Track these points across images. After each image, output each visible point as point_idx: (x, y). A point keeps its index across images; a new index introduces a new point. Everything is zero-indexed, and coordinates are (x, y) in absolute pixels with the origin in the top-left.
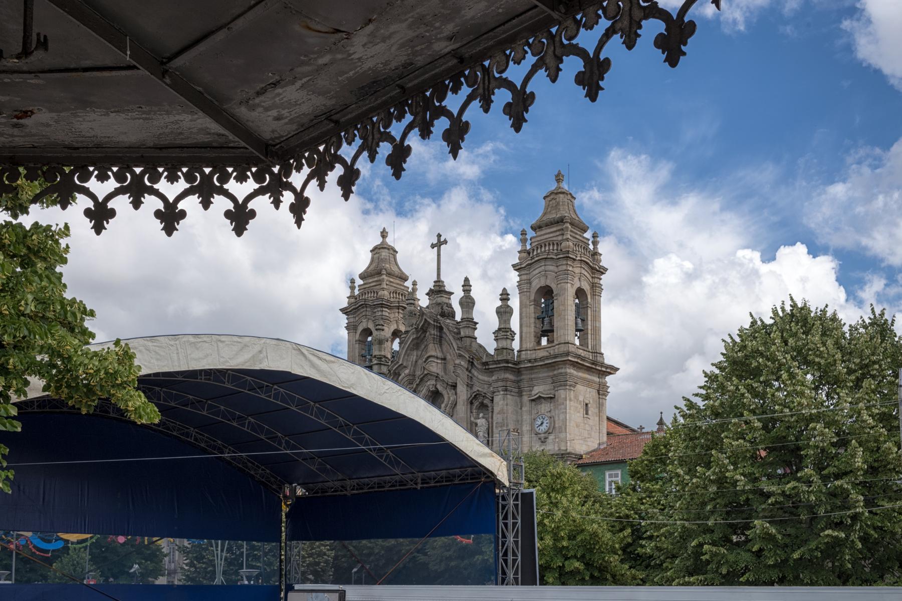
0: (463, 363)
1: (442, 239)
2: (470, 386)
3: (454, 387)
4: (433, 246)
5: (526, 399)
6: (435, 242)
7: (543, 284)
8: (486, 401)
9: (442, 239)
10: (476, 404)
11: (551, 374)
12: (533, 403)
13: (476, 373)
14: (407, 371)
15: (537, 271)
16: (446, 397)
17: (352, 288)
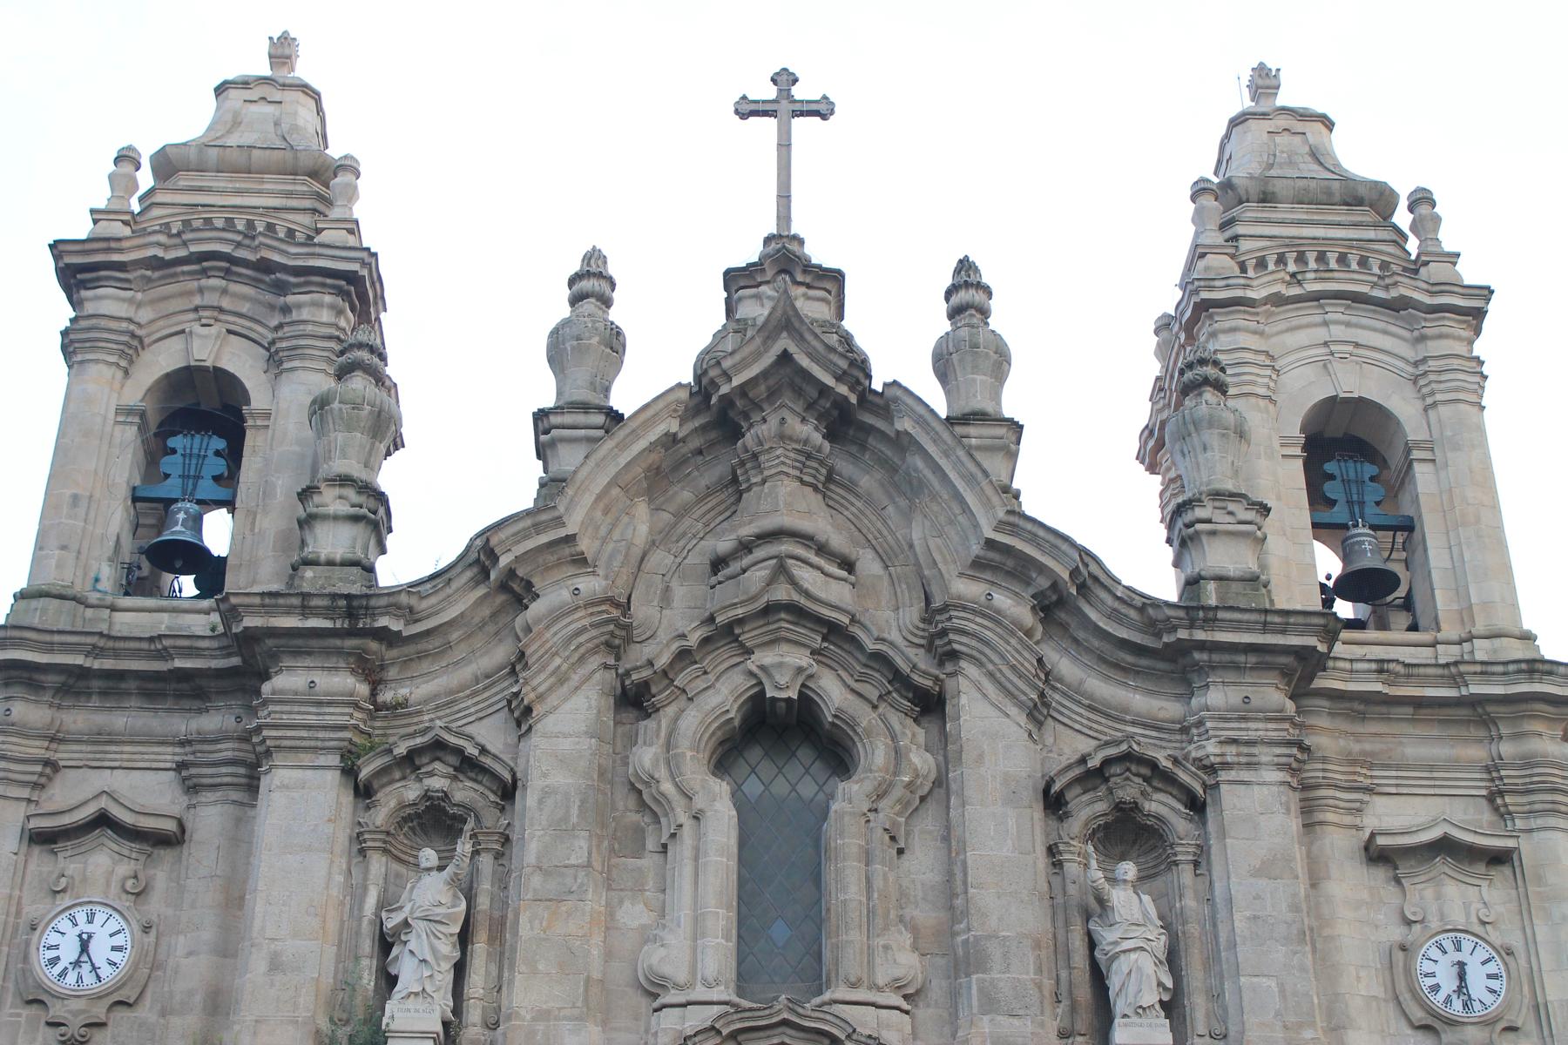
0: (1002, 600)
1: (798, 92)
2: (1038, 713)
3: (930, 705)
4: (748, 110)
5: (1339, 843)
6: (770, 92)
7: (1352, 383)
8: (1161, 805)
9: (798, 92)
10: (1087, 809)
11: (1477, 753)
12: (1381, 873)
13: (1066, 666)
14: (590, 585)
15: (1302, 337)
16: (874, 755)
17: (121, 182)
